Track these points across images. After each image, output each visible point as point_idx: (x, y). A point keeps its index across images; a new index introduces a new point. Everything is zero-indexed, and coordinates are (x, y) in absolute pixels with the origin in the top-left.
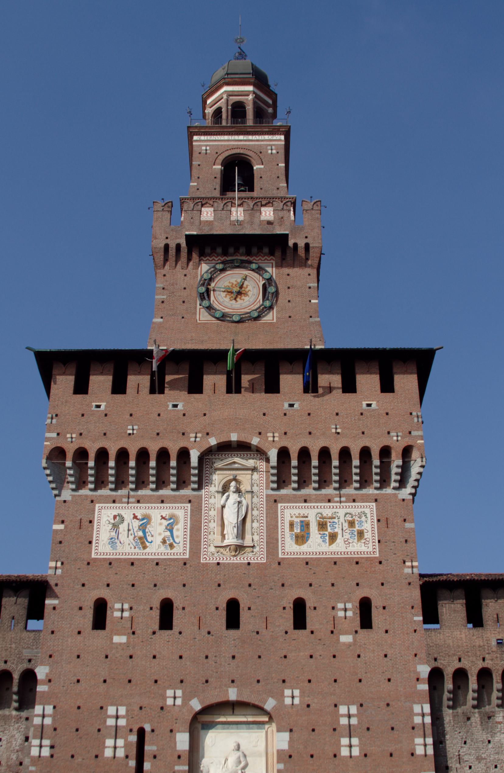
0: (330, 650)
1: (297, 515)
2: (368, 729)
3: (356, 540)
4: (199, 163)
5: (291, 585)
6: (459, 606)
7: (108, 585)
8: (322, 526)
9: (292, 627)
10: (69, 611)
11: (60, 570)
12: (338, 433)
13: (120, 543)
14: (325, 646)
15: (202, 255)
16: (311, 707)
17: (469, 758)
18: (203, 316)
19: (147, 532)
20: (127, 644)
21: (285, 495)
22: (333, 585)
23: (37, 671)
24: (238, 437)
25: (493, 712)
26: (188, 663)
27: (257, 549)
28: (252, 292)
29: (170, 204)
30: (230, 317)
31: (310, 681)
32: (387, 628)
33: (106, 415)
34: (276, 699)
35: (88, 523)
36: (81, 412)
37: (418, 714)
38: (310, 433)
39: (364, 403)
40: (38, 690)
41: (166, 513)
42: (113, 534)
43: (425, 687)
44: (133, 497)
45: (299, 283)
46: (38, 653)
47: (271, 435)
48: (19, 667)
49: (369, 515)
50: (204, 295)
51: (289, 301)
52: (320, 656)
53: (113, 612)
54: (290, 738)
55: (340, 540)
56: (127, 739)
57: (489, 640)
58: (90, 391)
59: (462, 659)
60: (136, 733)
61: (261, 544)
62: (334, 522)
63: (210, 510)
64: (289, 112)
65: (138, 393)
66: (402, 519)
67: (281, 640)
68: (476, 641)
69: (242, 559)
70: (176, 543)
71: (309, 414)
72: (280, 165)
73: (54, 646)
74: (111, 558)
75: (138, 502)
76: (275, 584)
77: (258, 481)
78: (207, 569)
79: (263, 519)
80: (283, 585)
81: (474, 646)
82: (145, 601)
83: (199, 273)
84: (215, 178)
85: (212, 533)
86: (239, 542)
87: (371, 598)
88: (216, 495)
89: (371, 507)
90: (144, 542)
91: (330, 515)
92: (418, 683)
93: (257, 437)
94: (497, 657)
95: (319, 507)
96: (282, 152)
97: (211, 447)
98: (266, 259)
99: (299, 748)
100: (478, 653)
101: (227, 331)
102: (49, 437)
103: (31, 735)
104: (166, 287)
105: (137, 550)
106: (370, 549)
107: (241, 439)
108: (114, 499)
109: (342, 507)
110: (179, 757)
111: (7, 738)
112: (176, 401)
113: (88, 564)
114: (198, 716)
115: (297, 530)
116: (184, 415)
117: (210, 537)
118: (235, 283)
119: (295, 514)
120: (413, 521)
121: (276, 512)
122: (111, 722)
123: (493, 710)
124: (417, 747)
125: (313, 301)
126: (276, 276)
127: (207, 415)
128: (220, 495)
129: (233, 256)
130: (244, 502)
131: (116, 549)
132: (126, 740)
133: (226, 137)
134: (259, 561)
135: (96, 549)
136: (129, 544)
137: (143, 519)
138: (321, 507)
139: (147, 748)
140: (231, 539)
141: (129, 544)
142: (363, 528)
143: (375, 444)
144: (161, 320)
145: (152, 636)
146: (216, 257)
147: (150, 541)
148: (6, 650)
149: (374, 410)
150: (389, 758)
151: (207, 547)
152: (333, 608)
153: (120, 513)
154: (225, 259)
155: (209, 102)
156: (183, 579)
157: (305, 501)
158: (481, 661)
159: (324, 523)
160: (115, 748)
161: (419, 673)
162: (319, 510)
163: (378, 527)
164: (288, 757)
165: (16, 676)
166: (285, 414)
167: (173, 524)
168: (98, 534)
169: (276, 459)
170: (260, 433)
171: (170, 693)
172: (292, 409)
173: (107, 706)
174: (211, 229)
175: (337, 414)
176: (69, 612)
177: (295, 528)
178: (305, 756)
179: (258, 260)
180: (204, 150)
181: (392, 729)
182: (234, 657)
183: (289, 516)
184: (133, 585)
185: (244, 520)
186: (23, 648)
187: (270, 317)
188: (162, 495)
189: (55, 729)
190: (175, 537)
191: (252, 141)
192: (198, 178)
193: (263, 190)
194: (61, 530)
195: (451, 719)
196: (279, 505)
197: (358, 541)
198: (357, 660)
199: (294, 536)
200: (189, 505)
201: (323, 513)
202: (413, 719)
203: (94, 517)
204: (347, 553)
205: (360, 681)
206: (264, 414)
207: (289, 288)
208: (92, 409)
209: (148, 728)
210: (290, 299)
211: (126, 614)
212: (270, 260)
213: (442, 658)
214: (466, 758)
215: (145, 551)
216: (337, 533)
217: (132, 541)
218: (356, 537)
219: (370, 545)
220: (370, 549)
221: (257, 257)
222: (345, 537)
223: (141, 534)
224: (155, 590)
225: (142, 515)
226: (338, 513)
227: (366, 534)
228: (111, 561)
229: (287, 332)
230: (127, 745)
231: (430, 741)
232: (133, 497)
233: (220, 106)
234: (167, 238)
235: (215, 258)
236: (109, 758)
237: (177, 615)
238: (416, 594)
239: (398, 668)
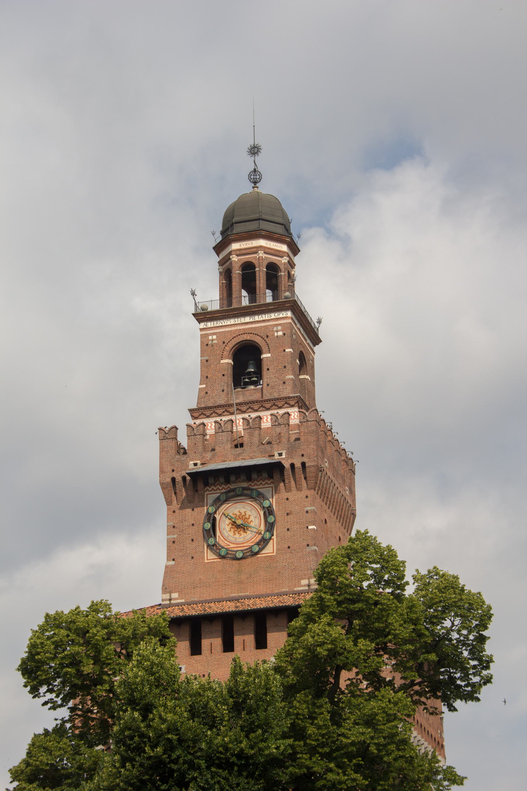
4: (206, 358)
15: (206, 484)
18: (210, 556)
28: (254, 523)
45: (297, 507)
72: (287, 350)
98: (266, 483)
104: (176, 525)
118: (238, 514)
133: (232, 321)
144: (173, 563)
154: (229, 487)
179: (259, 485)
187: (270, 549)
192: (207, 377)
207: (288, 514)
212: (270, 484)
221: (258, 482)
234: (173, 471)
235: (218, 486)
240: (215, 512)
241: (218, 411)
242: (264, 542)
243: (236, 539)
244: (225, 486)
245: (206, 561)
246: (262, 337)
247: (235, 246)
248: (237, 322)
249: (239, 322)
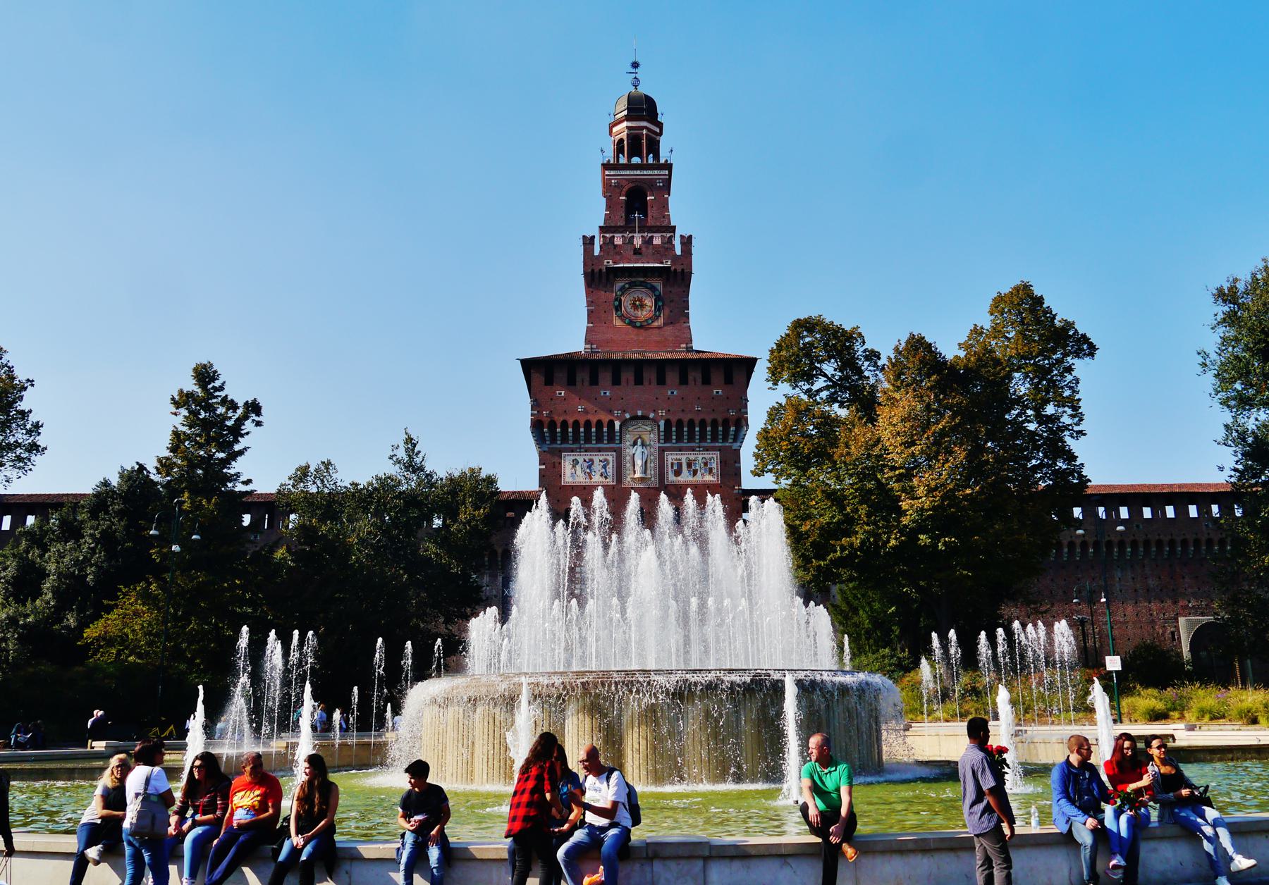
8: (689, 465)
15: (616, 276)
18: (618, 323)
27: (653, 479)
41: (601, 458)
55: (699, 473)
64: (672, 151)
115: (675, 468)
117: (628, 472)
128: (631, 448)
130: (646, 452)
133: (628, 172)
140: (638, 475)
155: (615, 130)
185: (646, 462)
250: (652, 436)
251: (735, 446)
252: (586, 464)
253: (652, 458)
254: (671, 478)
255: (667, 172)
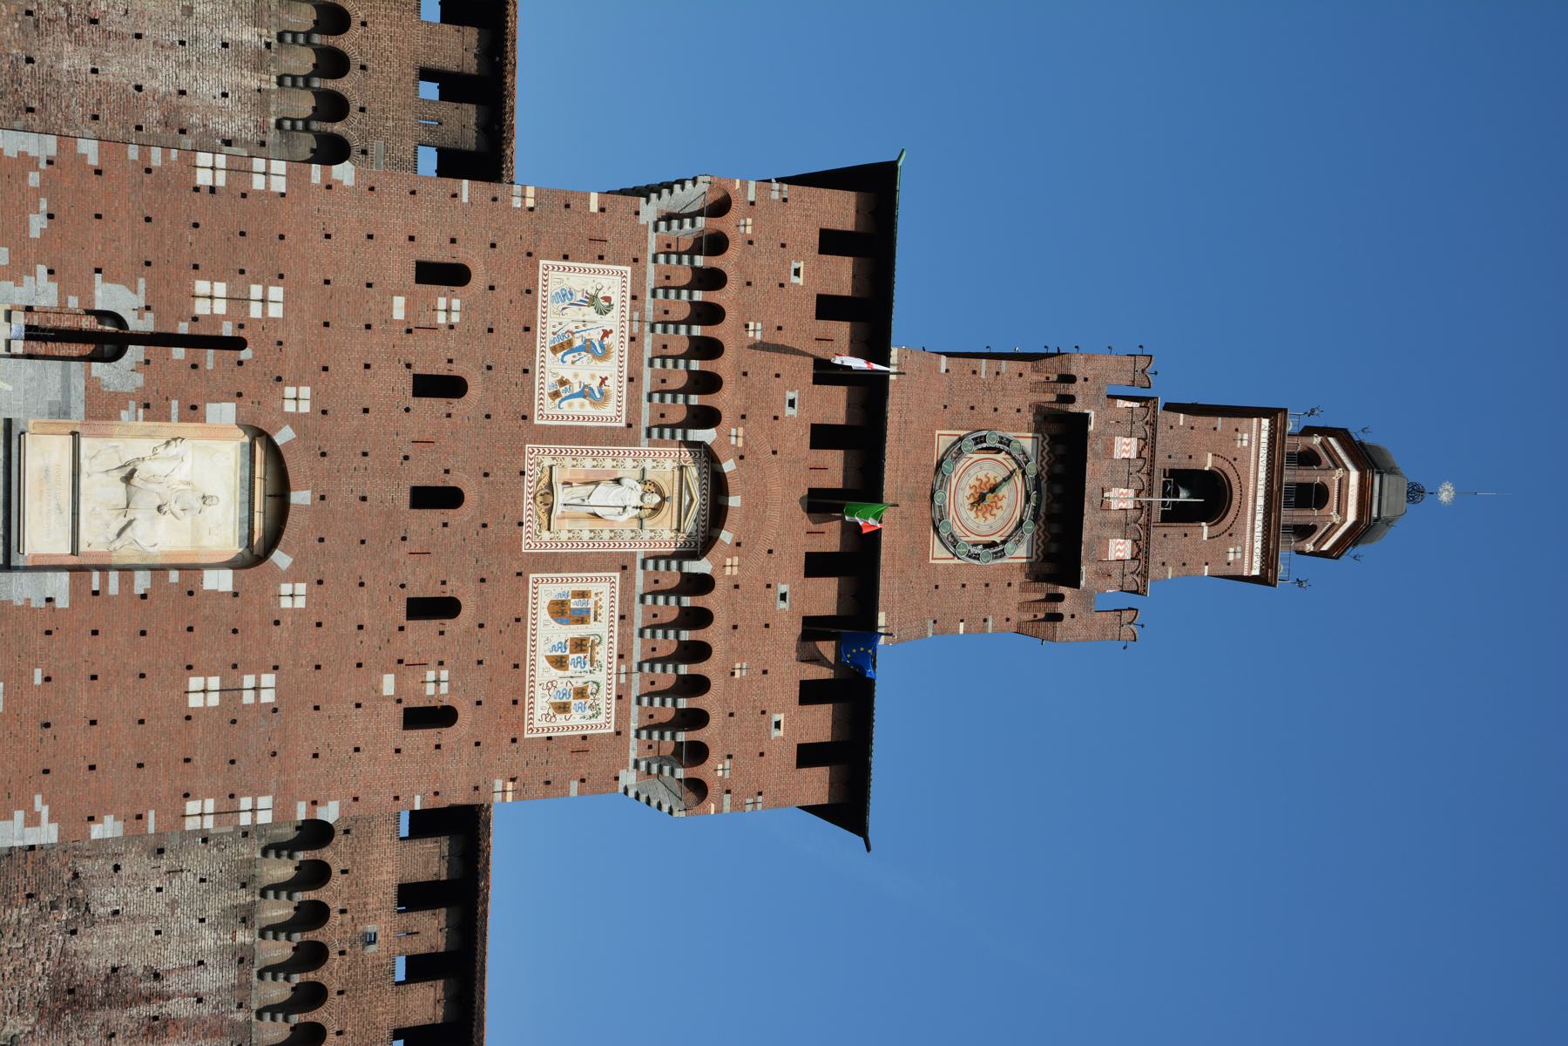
0: (371, 658)
1: (600, 603)
2: (234, 722)
3: (553, 700)
4: (1219, 428)
5: (482, 593)
6: (436, 869)
7: (492, 288)
8: (579, 645)
9: (412, 596)
10: (449, 220)
11: (519, 206)
12: (733, 674)
13: (564, 309)
14: (377, 650)
15: (1054, 440)
16: (274, 627)
17: (175, 888)
18: (944, 439)
19: (579, 354)
20: (389, 321)
21: (634, 583)
22: (480, 662)
23: (347, 162)
24: (734, 507)
25: (252, 927)
26: (355, 423)
27: (546, 535)
29: (1147, 384)
30: (941, 485)
31: (319, 625)
32: (404, 752)
33: (782, 285)
34: (290, 570)
35: (599, 253)
36: (788, 242)
37: (255, 803)
38: (735, 627)
39: (780, 717)
40: (313, 165)
41: (612, 384)
42: (579, 297)
43: (302, 813)
44: (641, 329)
45: (994, 601)
46: (378, 166)
47: (736, 563)
48: (352, 133)
49: (593, 721)
50: (981, 442)
51: (964, 586)
52: (362, 642)
53: (445, 295)
54: (222, 593)
55: (555, 673)
56: (226, 320)
57: (375, 920)
58: (824, 257)
59: (346, 875)
60: (237, 335)
61: (553, 544)
62: (585, 664)
63: (613, 460)
65: (816, 339)
66: (585, 777)
67: (390, 577)
68: (376, 898)
69: (530, 512)
70: (560, 402)
71: (767, 626)
72: (1206, 567)
73: (389, 194)
74: (537, 293)
75: (632, 339)
76: (485, 568)
77: (659, 539)
78: (514, 454)
79: (596, 547)
80: (483, 580)
81: (367, 895)
82: (463, 351)
83: (1021, 434)
84: (1190, 457)
85: (575, 463)
86: (558, 510)
87: (456, 726)
88: (640, 468)
89: (608, 725)
90: (564, 349)
91: (597, 657)
92: (310, 803)
93: (733, 538)
94: (345, 932)
95: (611, 640)
96: (1231, 572)
97: (720, 463)
98: (1039, 547)
99: (205, 608)
100: (354, 902)
101: (917, 482)
102: (748, 187)
103: (234, 150)
104: (999, 377)
105: (550, 337)
106: (537, 724)
107: (729, 512)
108: (639, 298)
109: (609, 677)
110: (194, 408)
111: (228, 107)
112: (799, 404)
113: (529, 254)
114: (264, 437)
115: (574, 604)
116: (776, 418)
117: (568, 461)
119: (600, 600)
120: (580, 793)
121: (606, 569)
122: (256, 291)
123: (257, 926)
124: (200, 801)
125: (962, 624)
126: (1007, 564)
127: (773, 456)
128: (638, 476)
129: (1048, 491)
130: (625, 517)
131: (552, 302)
132: (224, 317)
133: (1262, 475)
134: (524, 541)
135: (554, 268)
136: (560, 324)
137: (602, 347)
138: (611, 642)
139: (210, 352)
140: (561, 495)
141: (560, 324)
142: (573, 711)
143: (712, 734)
144: (943, 370)
145: (402, 363)
146: (1047, 463)
147: (565, 360)
148: (383, 110)
149: (769, 731)
150: (182, 757)
151: (552, 454)
152: (441, 663)
153: (615, 307)
154: (1043, 478)
156: (500, 414)
157: (622, 617)
158: (340, 907)
159: (584, 648)
160: (211, 297)
161: (325, 804)
162: (605, 640)
163: (575, 736)
164: (189, 589)
165: (337, 128)
166: (769, 586)
167: (590, 396)
168: (580, 270)
169: (694, 571)
170: (738, 544)
171: (305, 392)
172: (776, 598)
173: (284, 286)
174: (1096, 454)
175: (765, 672)
176: (446, 221)
177: (577, 600)
178: (192, 617)
180: (1242, 436)
181: (233, 762)
182: (364, 499)
183: (599, 591)
184: (490, 330)
185: (595, 515)
186: (386, 140)
187: (939, 553)
188: (642, 379)
189: (244, 196)
190: (570, 400)
191: (1253, 520)
192: (1192, 428)
193: (1162, 538)
194: (589, 207)
195: (245, 856)
196: (617, 575)
197: (551, 703)
198: (352, 702)
199: (564, 598)
200: (623, 424)
201: (600, 646)
202: (248, 796)
203: (608, 263)
204: (532, 686)
205: (317, 708)
206: (770, 552)
208: (793, 262)
209: (245, 354)
210: (967, 586)
211: (441, 318)
212: (1037, 554)
213: (349, 841)
214: (176, 882)
215: (548, 350)
216: (567, 670)
217: (566, 329)
218: (558, 700)
219: (546, 725)
220: (537, 724)
221: (1043, 532)
222: (559, 681)
223: (578, 343)
224: (482, 367)
225: (609, 346)
226: (601, 670)
227: (563, 716)
228: (533, 293)
229: (911, 582)
230: (215, 319)
231: (209, 823)
232: (641, 329)
233: (1323, 463)
235: (1047, 459)
236: (194, 288)
237: (438, 405)
238: (460, 799)
239: (335, 770)
240: (1007, 453)
241: (1146, 450)
242: (952, 543)
243: (963, 489)
244: (1045, 471)
245: (937, 432)
246: (1231, 525)
247: (1354, 476)
248: (1259, 483)
249: (1259, 487)
250: (668, 535)
251: (628, 778)
252: (595, 336)
253: (606, 535)
254: (546, 590)
255: (1256, 572)
